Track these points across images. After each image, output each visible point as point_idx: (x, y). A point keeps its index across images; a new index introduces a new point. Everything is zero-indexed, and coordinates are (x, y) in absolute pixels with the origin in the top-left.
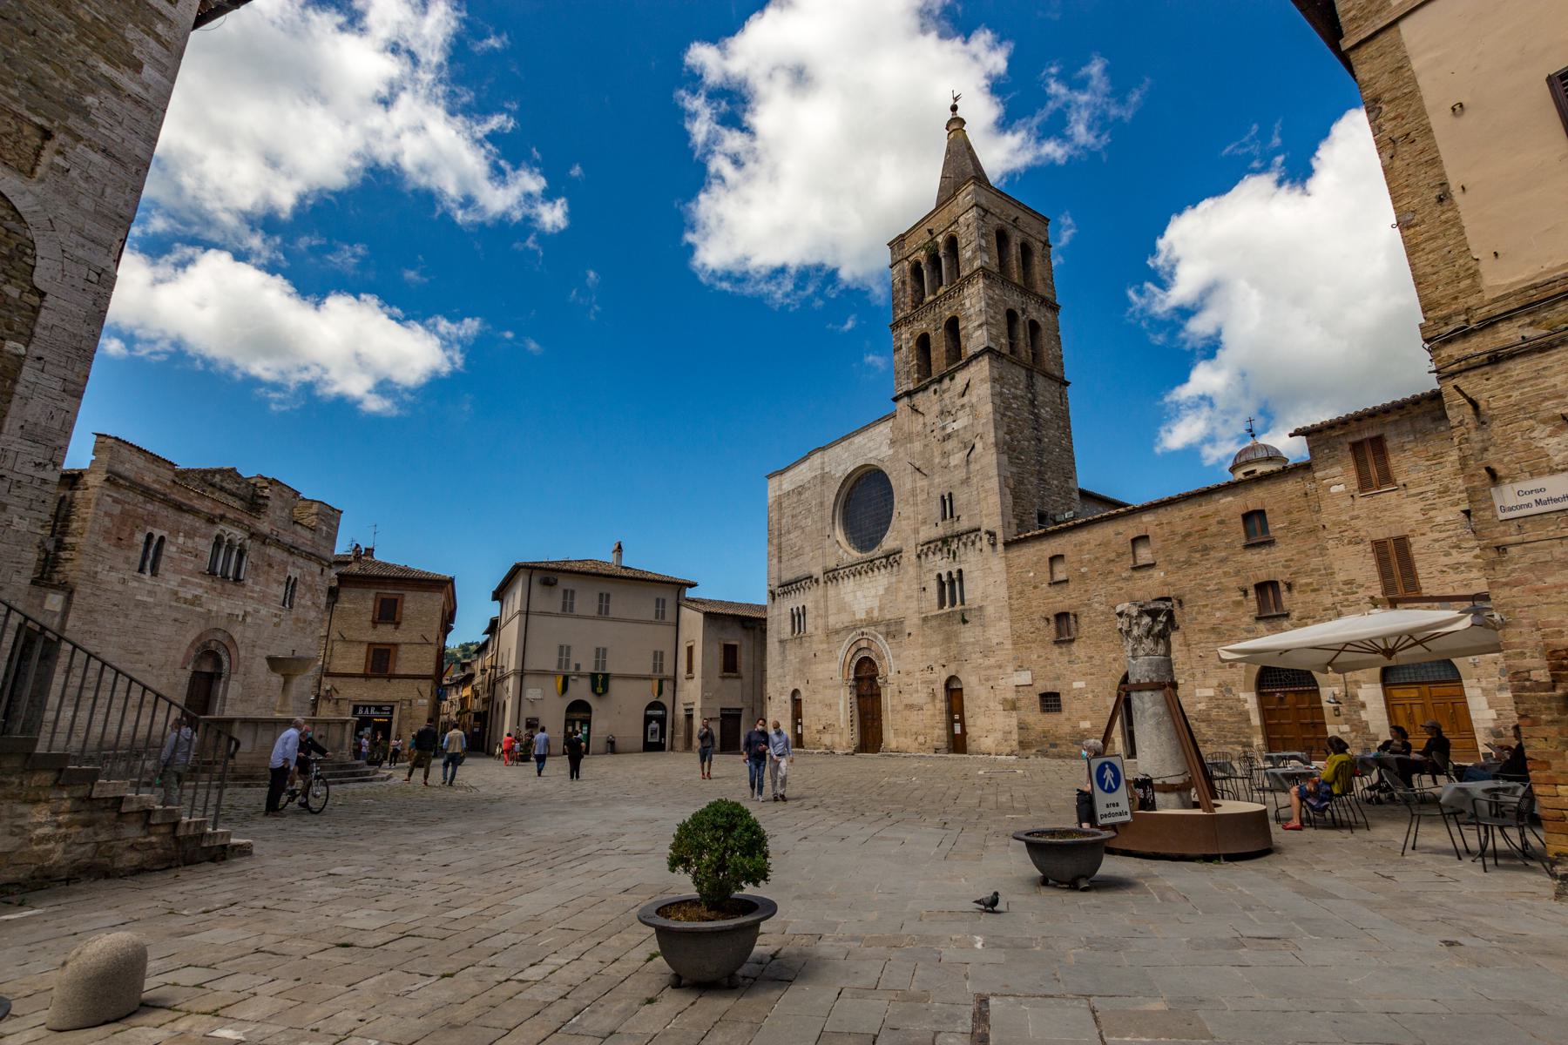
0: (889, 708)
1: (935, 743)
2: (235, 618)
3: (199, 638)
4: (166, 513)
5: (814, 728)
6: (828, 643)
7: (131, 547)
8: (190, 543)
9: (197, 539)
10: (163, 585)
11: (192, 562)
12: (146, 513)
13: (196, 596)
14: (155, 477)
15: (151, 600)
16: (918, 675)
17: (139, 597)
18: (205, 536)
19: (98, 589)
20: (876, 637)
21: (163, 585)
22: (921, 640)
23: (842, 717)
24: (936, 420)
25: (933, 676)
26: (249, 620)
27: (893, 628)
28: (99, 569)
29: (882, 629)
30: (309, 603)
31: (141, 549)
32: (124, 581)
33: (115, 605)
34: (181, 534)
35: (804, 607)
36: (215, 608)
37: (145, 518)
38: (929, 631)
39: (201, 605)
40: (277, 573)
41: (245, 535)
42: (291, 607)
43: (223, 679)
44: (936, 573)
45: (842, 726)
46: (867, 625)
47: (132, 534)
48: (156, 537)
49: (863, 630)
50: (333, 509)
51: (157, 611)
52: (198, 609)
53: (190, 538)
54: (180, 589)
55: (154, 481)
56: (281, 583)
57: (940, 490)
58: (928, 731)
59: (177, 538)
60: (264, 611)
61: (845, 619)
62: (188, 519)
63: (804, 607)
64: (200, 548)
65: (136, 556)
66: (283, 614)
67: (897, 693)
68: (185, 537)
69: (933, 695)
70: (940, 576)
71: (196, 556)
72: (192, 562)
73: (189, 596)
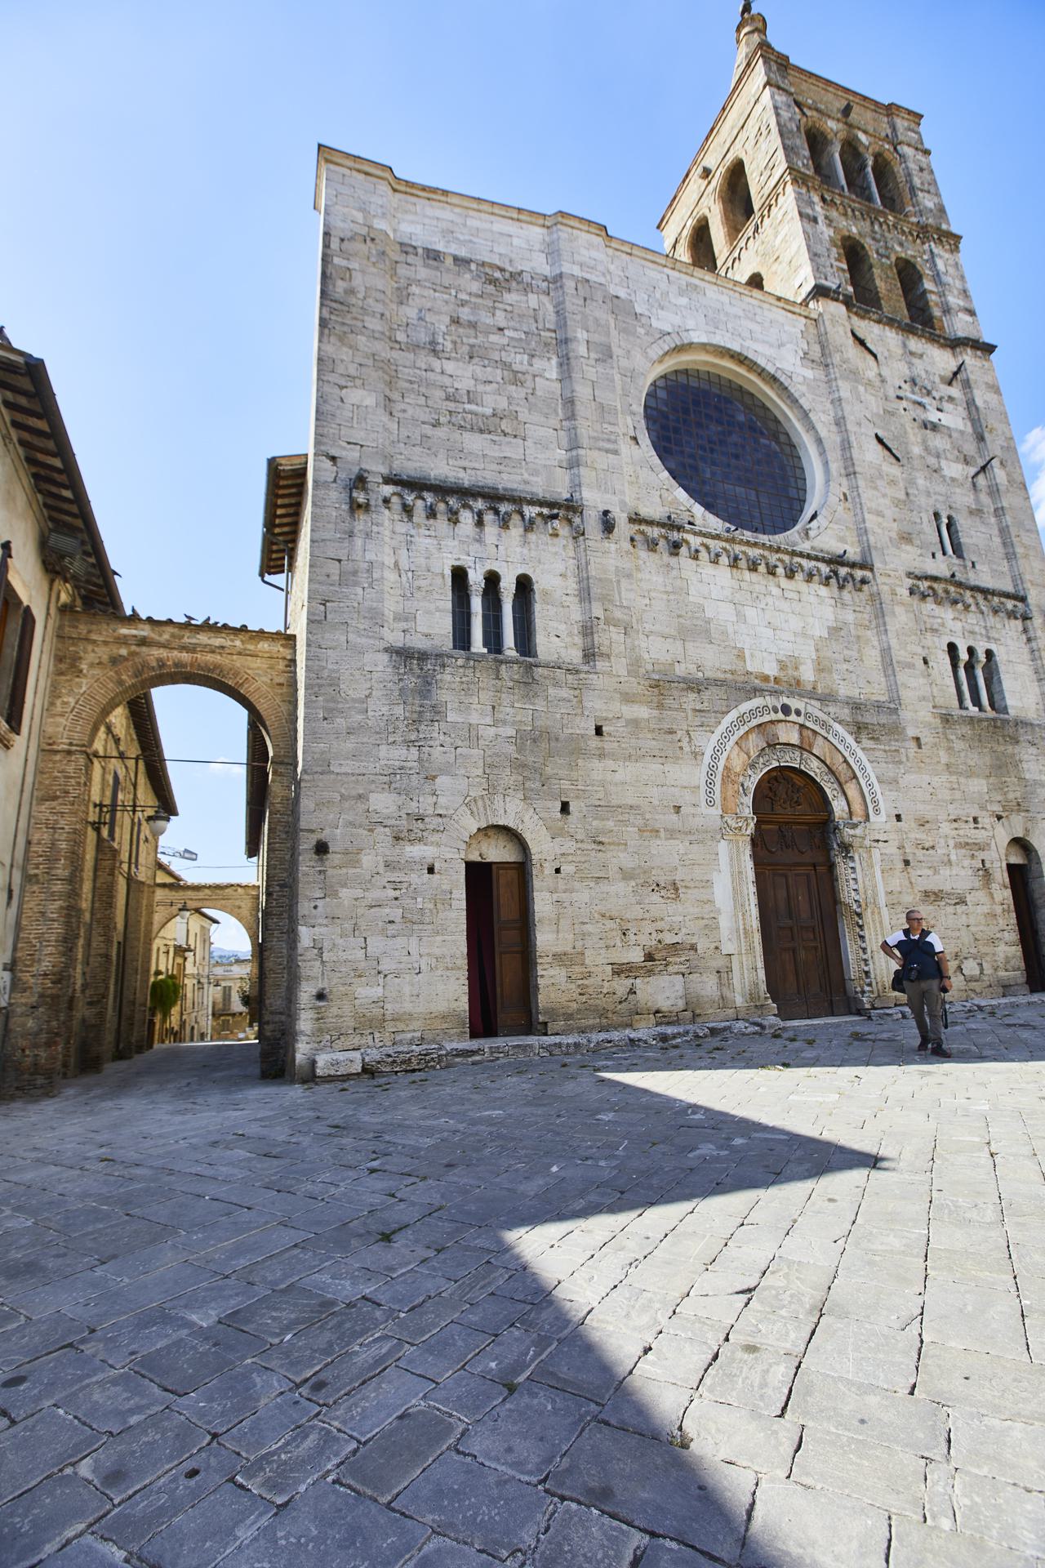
0: (882, 900)
1: (1002, 973)
5: (598, 960)
6: (660, 706)
16: (946, 828)
20: (824, 724)
22: (944, 758)
23: (725, 923)
24: (905, 386)
25: (981, 836)
27: (869, 718)
29: (845, 713)
38: (959, 745)
44: (946, 640)
45: (727, 948)
46: (791, 694)
49: (786, 700)
57: (931, 501)
58: (984, 950)
61: (710, 660)
67: (901, 865)
69: (985, 873)
70: (952, 648)
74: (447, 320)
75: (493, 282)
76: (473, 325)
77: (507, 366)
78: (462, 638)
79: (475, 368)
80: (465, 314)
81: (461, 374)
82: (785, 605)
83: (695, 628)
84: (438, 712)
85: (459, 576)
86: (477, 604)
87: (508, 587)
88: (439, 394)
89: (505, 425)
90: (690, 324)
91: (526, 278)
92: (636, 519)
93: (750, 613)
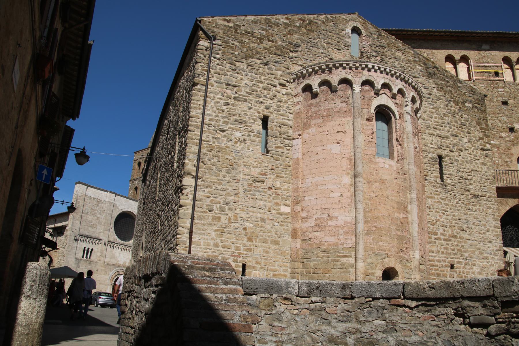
6: (106, 268)
35: (92, 249)
61: (114, 261)
63: (92, 249)
74: (90, 208)
75: (98, 202)
76: (94, 209)
77: (97, 216)
78: (83, 257)
79: (93, 217)
80: (93, 208)
81: (91, 218)
82: (126, 254)
83: (113, 257)
84: (79, 267)
85: (85, 248)
86: (86, 252)
87: (90, 250)
88: (87, 221)
89: (95, 226)
90: (125, 207)
91: (103, 201)
92: (109, 242)
93: (121, 255)
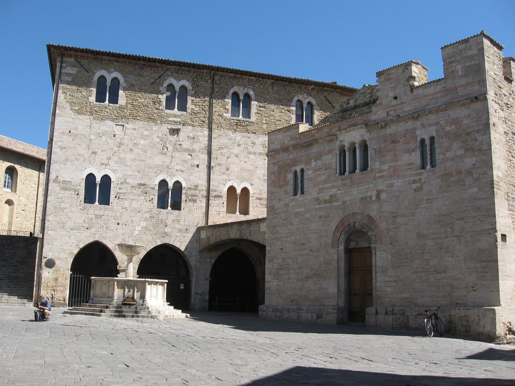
2: (368, 199)
3: (342, 222)
4: (300, 154)
7: (286, 183)
8: (319, 163)
9: (323, 158)
10: (308, 197)
11: (323, 174)
12: (290, 161)
13: (331, 196)
14: (289, 139)
15: (303, 209)
17: (296, 211)
18: (330, 152)
19: (276, 214)
21: (308, 197)
26: (383, 196)
28: (274, 203)
30: (461, 152)
31: (292, 182)
32: (287, 205)
33: (285, 220)
34: (313, 160)
36: (347, 198)
37: (290, 164)
39: (336, 201)
40: (406, 143)
41: (363, 131)
42: (433, 165)
43: (373, 251)
47: (285, 177)
48: (298, 171)
50: (466, 41)
51: (308, 215)
52: (335, 204)
53: (319, 160)
54: (319, 196)
55: (290, 141)
56: (414, 150)
59: (310, 164)
60: (398, 183)
62: (315, 149)
64: (327, 162)
65: (290, 188)
66: (424, 177)
68: (315, 161)
71: (326, 170)
72: (323, 174)
73: (327, 198)
